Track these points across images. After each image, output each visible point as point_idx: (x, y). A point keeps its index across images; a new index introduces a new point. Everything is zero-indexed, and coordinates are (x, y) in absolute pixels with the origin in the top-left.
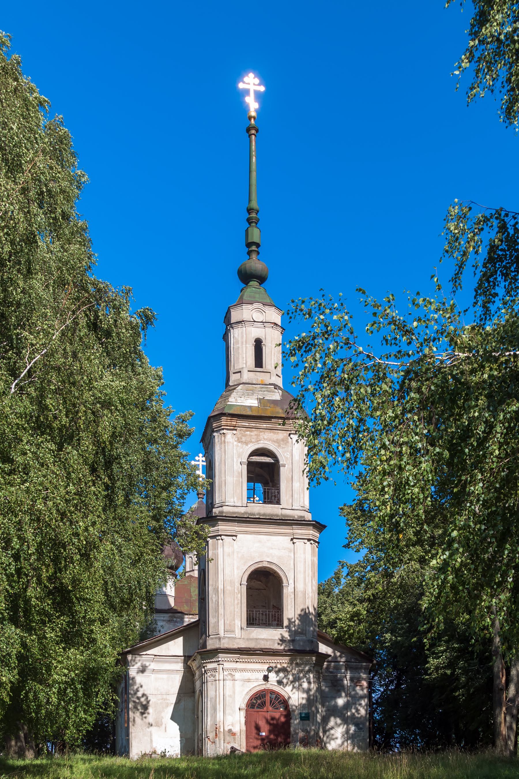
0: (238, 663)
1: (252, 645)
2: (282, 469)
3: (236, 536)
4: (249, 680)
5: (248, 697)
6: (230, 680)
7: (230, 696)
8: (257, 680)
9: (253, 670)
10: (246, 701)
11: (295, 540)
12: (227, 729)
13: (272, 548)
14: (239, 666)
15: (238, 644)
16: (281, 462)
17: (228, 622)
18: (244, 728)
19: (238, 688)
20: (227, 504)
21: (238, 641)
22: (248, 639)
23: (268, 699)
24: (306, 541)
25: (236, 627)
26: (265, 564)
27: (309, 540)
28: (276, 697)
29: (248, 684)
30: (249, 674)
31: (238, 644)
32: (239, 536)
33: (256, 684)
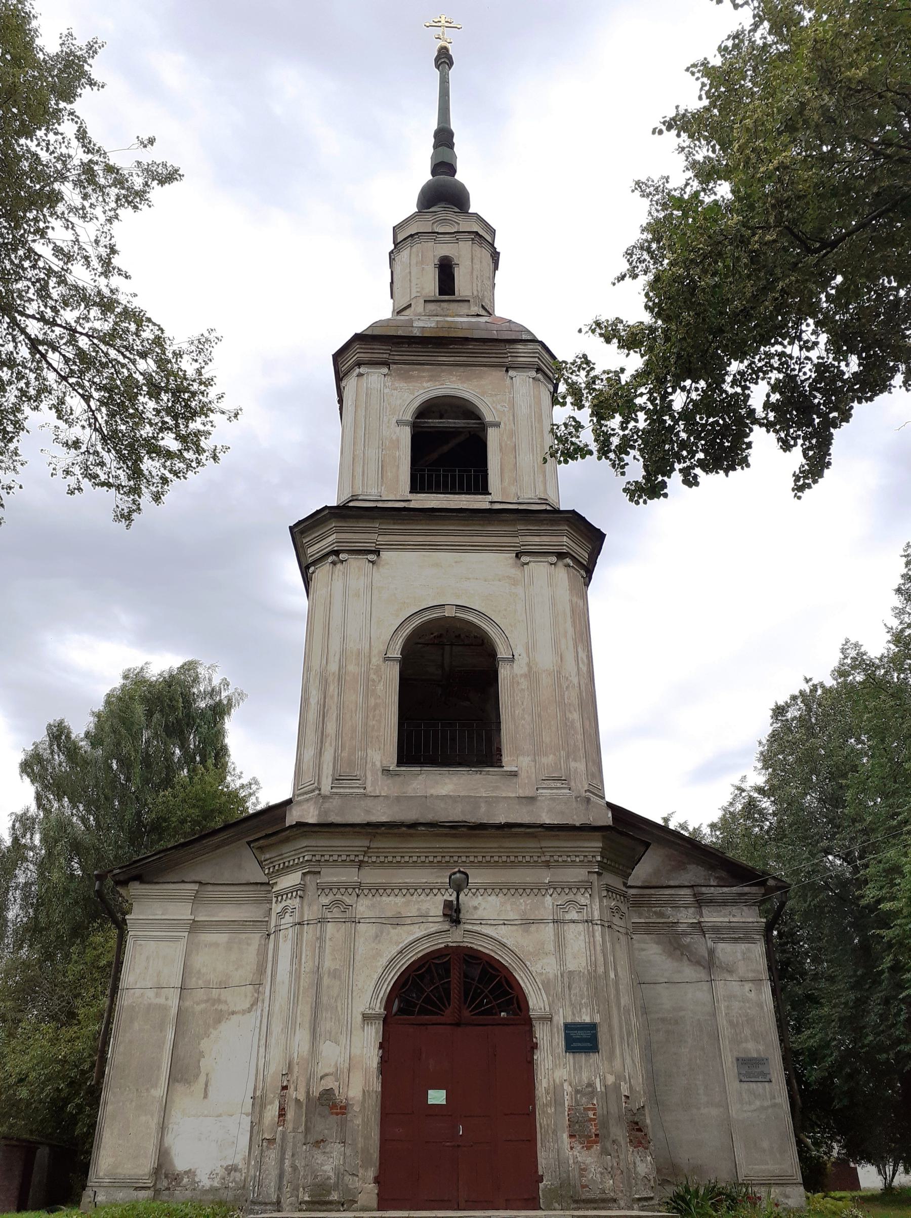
0: (366, 871)
1: (411, 816)
3: (377, 552)
4: (397, 921)
6: (336, 921)
7: (335, 974)
8: (423, 917)
9: (411, 889)
10: (386, 988)
11: (525, 559)
14: (371, 876)
15: (368, 812)
16: (488, 418)
17: (345, 754)
19: (363, 948)
20: (360, 498)
21: (369, 802)
22: (398, 799)
23: (455, 977)
24: (554, 559)
25: (369, 766)
26: (449, 613)
27: (561, 556)
29: (393, 932)
30: (400, 900)
31: (368, 812)
32: (383, 554)
33: (418, 932)
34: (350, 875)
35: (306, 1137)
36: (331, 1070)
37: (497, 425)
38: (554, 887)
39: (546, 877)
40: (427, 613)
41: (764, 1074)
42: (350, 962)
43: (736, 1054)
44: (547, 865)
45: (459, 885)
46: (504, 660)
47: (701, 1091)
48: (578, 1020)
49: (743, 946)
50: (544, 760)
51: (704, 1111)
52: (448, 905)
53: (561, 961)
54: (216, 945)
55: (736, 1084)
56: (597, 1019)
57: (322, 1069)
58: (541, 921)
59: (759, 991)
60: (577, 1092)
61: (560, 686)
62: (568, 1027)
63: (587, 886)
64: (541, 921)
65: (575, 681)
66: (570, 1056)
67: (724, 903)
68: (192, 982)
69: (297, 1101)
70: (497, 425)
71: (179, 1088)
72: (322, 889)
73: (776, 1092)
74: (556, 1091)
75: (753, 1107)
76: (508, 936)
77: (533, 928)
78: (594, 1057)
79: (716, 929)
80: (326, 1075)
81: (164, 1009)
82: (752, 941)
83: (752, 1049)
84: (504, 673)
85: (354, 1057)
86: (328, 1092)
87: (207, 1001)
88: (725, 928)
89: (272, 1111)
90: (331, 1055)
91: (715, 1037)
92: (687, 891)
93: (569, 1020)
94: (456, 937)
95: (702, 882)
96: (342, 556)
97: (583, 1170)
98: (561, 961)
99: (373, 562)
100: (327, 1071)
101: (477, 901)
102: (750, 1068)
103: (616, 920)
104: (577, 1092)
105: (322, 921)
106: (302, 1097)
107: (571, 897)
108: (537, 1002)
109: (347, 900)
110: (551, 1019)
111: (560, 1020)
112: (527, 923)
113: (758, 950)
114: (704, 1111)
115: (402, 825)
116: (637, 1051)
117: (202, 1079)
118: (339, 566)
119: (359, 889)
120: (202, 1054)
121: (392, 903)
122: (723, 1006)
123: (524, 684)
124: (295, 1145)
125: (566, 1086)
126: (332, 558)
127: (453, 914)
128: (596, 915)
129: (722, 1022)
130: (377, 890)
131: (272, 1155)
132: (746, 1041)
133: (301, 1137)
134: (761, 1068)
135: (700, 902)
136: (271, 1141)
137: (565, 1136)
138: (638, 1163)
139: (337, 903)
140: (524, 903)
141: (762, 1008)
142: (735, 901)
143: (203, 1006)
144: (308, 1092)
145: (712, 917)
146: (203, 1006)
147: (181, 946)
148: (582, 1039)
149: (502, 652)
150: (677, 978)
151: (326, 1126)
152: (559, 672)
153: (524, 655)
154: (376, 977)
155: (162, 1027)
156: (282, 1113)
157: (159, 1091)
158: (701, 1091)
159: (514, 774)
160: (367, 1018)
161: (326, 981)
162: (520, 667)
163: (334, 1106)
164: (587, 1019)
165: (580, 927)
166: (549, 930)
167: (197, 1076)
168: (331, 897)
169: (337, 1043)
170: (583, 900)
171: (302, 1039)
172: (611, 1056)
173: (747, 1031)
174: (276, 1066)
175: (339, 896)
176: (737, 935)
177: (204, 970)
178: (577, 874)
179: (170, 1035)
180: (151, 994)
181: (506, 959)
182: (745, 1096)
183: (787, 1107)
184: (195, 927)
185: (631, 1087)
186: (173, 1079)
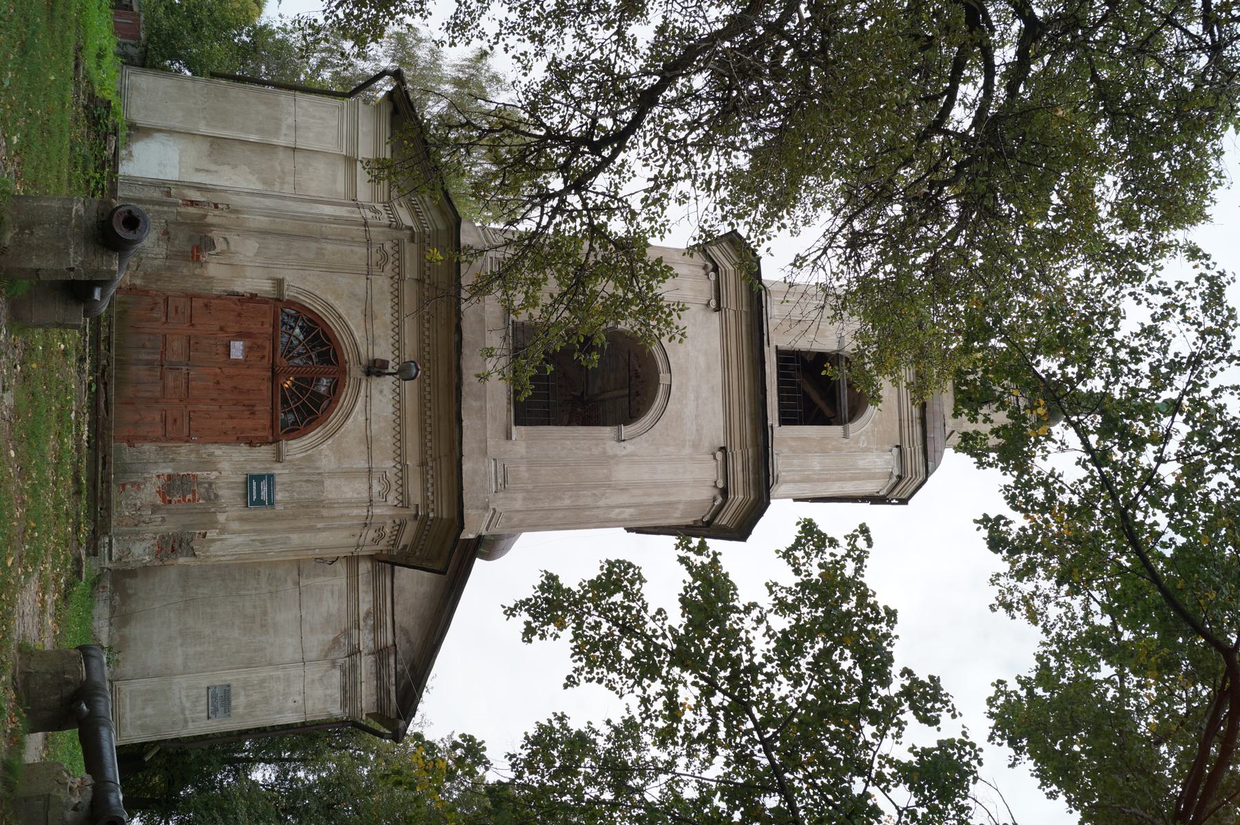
2: (840, 428)
3: (718, 309)
4: (369, 315)
5: (318, 308)
6: (369, 256)
9: (398, 329)
10: (307, 301)
11: (719, 455)
12: (215, 235)
13: (697, 398)
16: (851, 426)
18: (218, 289)
19: (343, 281)
24: (721, 485)
27: (724, 492)
28: (321, 397)
29: (358, 312)
30: (388, 318)
32: (716, 316)
33: (359, 335)
34: (410, 271)
35: (172, 223)
36: (232, 248)
37: (846, 436)
38: (403, 467)
39: (412, 462)
40: (662, 356)
41: (215, 711)
42: (331, 269)
43: (234, 684)
44: (423, 464)
45: (404, 373)
46: (620, 431)
47: (199, 649)
48: (278, 488)
49: (338, 695)
50: (523, 468)
51: (180, 651)
52: (384, 364)
53: (332, 474)
54: (335, 181)
55: (205, 684)
56: (279, 507)
57: (233, 238)
58: (370, 458)
59: (295, 711)
60: (210, 484)
61: (595, 487)
62: (271, 477)
63: (404, 503)
64: (370, 458)
65: (602, 503)
66: (241, 479)
67: (379, 678)
68: (300, 158)
69: (205, 216)
70: (846, 436)
71: (205, 147)
72: (398, 244)
73: (199, 724)
74: (208, 463)
75: (184, 699)
76: (358, 416)
77: (364, 448)
78: (240, 501)
79: (354, 667)
80: (228, 243)
81: (277, 132)
82: (344, 704)
83: (239, 701)
84: (607, 431)
85: (243, 269)
86: (212, 245)
87: (283, 172)
88: (355, 678)
89: (195, 196)
90: (247, 249)
91: (250, 664)
92: (390, 642)
93: (277, 479)
94: (355, 371)
95: (400, 656)
96: (712, 275)
97: (137, 485)
98: (332, 474)
99: (708, 305)
100: (232, 243)
101: (388, 393)
102: (221, 699)
103: (372, 534)
104: (210, 484)
105: (369, 242)
106: (210, 219)
107: (394, 486)
108: (294, 448)
109: (388, 267)
110: (278, 461)
111: (277, 469)
112: (369, 442)
113: (336, 711)
114: (180, 651)
115: (460, 319)
116: (247, 550)
117: (213, 167)
118: (703, 272)
119: (398, 278)
120: (235, 167)
121: (385, 311)
122: (280, 673)
123: (596, 451)
124: (165, 213)
125: (214, 474)
126: (710, 266)
127: (375, 369)
128: (377, 511)
129: (264, 673)
130: (397, 297)
131: (157, 194)
132: (247, 696)
133: (172, 217)
134: (221, 709)
135: (381, 654)
136: (169, 194)
137: (170, 471)
138: (144, 544)
139: (385, 258)
140: (386, 441)
141: (278, 713)
142: (381, 689)
143: (279, 168)
144: (213, 225)
145: (366, 665)
146: (279, 168)
147: (332, 147)
148: (257, 490)
149: (626, 430)
150: (306, 628)
151: (182, 241)
152: (609, 486)
153: (625, 452)
154: (317, 293)
155: (260, 131)
156: (193, 203)
157: (203, 129)
158: (199, 649)
159: (508, 436)
160: (279, 283)
161: (313, 245)
162: (612, 447)
163: (199, 249)
164: (279, 496)
165: (365, 495)
166: (363, 464)
167: (216, 163)
168: (390, 252)
169: (257, 254)
170: (391, 499)
171: (261, 222)
172: (242, 519)
173: (256, 697)
174: (235, 200)
175: (391, 259)
176: (349, 692)
177: (311, 169)
178: (416, 496)
179: (253, 138)
180: (290, 120)
181: (335, 418)
182: (195, 691)
183: (184, 733)
184: (351, 161)
185: (214, 541)
186: (215, 141)
